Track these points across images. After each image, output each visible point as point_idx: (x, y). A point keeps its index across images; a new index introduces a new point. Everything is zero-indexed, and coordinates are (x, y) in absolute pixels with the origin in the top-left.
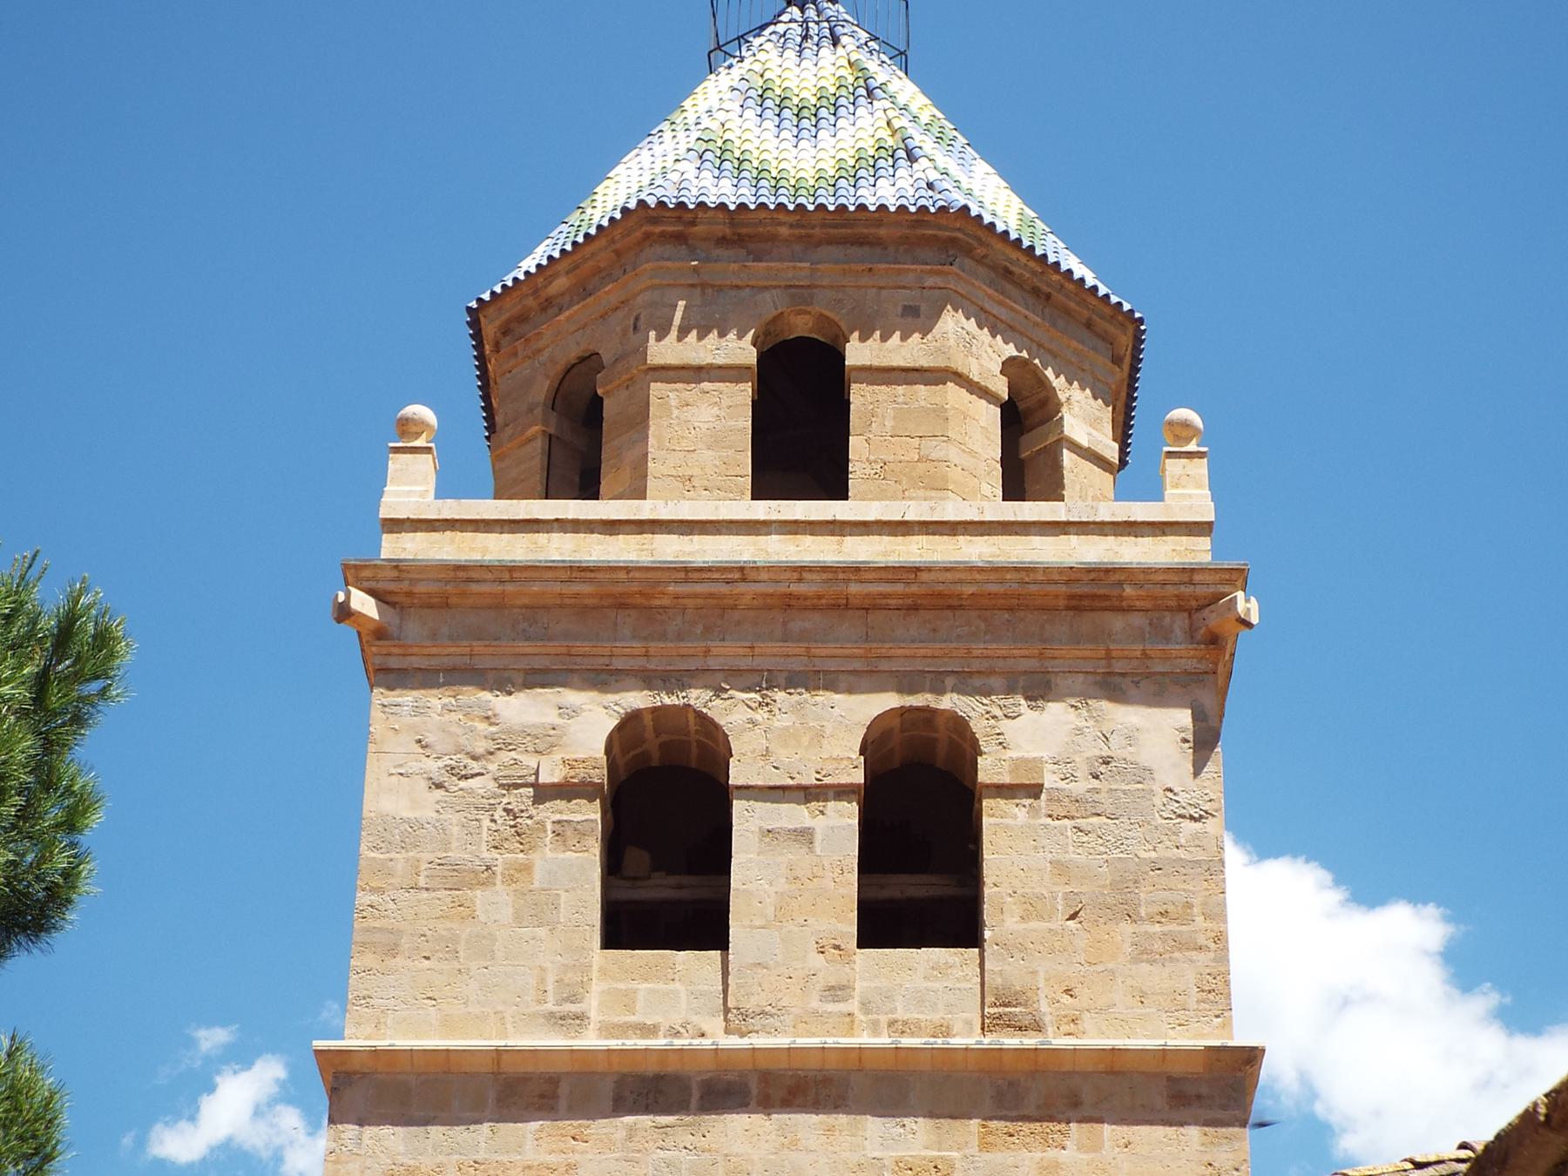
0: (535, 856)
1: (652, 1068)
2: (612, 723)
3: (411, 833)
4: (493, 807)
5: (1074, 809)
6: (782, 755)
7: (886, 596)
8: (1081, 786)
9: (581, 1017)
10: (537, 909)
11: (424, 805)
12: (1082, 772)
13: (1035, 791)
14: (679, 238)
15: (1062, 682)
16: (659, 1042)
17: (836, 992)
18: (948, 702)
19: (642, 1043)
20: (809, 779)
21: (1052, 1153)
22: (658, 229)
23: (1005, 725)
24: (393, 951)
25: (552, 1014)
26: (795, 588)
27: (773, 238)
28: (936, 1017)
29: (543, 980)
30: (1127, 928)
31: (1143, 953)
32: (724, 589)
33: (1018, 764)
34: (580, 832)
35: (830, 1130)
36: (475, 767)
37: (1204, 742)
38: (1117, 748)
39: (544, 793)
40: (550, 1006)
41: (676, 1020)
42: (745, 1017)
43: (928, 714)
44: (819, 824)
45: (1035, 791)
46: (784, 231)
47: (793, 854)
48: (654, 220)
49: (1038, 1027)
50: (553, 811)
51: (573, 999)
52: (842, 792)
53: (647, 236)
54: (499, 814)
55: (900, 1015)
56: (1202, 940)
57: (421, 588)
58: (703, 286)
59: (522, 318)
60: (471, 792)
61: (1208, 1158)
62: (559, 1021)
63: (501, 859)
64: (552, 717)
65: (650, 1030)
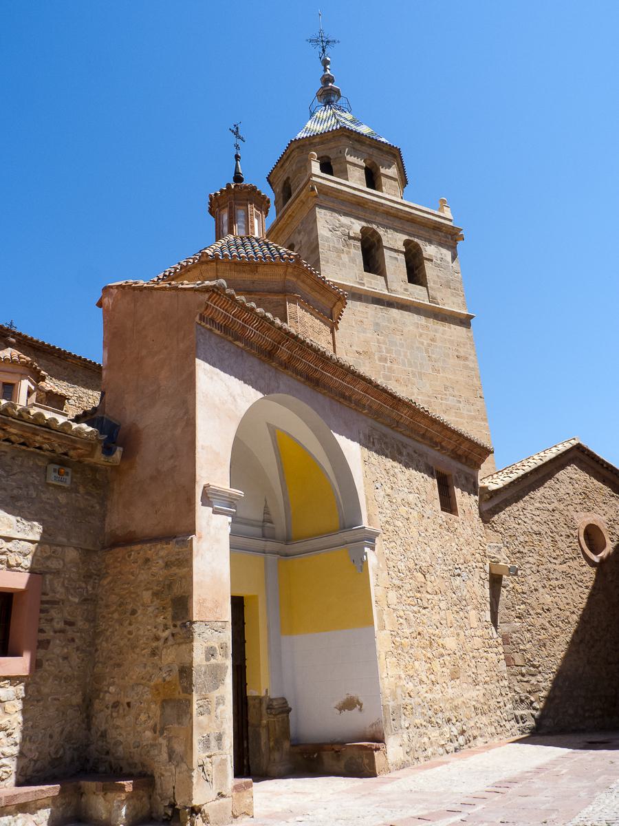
1: (377, 297)
2: (360, 228)
5: (438, 266)
7: (404, 217)
8: (439, 262)
9: (363, 284)
10: (353, 260)
11: (329, 234)
13: (432, 261)
14: (348, 137)
15: (434, 242)
17: (406, 290)
18: (416, 240)
19: (373, 290)
20: (396, 248)
24: (328, 262)
26: (391, 211)
27: (365, 143)
28: (422, 299)
32: (378, 207)
35: (409, 316)
37: (454, 258)
39: (350, 238)
40: (358, 280)
43: (412, 241)
45: (432, 261)
46: (367, 142)
47: (395, 262)
50: (352, 242)
51: (362, 280)
52: (401, 252)
57: (324, 190)
58: (354, 148)
59: (303, 146)
63: (345, 249)
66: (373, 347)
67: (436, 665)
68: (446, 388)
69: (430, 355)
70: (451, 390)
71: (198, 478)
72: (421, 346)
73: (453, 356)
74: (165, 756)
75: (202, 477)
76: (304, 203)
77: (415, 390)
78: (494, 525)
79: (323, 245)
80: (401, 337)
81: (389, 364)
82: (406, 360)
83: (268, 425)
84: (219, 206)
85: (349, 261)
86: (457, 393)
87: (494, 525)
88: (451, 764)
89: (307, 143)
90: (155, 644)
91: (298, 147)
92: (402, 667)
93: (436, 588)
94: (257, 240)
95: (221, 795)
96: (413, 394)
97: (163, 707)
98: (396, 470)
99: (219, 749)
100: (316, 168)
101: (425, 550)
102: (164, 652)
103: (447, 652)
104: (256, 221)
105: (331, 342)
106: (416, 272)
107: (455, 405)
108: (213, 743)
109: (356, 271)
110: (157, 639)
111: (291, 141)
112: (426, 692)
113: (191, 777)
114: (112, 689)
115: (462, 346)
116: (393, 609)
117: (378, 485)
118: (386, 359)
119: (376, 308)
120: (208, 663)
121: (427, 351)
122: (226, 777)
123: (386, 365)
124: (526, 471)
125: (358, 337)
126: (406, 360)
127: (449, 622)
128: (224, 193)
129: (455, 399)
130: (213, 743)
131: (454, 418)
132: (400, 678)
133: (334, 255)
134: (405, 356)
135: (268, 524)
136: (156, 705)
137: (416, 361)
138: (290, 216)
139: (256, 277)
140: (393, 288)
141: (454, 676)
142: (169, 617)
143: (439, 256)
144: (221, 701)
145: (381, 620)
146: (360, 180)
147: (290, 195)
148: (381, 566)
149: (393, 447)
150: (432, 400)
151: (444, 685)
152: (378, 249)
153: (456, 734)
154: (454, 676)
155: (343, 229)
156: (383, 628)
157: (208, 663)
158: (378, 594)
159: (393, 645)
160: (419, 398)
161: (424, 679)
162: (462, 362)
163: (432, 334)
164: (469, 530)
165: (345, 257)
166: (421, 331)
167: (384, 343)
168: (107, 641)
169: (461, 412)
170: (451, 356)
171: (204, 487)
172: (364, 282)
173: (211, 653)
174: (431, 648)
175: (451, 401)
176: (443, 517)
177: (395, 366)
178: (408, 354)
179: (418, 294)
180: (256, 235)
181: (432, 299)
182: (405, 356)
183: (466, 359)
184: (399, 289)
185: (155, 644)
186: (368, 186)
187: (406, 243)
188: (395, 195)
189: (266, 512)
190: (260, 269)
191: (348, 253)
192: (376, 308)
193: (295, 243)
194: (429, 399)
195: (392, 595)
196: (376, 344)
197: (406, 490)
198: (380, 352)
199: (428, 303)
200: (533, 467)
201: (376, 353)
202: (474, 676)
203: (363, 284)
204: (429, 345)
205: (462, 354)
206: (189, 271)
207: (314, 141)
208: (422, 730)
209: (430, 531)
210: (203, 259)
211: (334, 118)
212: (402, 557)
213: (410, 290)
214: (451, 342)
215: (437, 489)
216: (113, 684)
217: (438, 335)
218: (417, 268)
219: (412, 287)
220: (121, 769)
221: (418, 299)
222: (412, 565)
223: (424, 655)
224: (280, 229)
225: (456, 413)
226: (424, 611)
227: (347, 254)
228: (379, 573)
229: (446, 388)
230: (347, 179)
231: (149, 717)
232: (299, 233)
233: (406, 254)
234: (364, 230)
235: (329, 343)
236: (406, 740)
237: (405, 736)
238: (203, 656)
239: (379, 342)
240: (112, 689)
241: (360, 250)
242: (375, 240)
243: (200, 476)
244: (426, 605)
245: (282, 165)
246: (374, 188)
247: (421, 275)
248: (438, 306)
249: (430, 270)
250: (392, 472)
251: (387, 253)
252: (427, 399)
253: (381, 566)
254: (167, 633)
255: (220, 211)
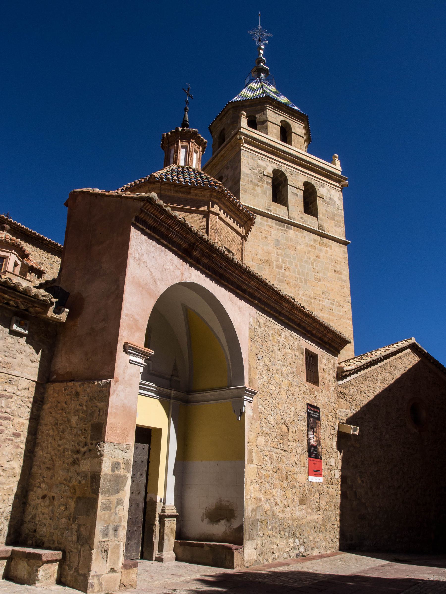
0: (264, 185)
3: (247, 175)
4: (258, 176)
5: (327, 203)
6: (294, 182)
8: (328, 200)
9: (271, 210)
10: (265, 193)
11: (249, 172)
12: (328, 198)
16: (280, 217)
17: (302, 218)
21: (327, 249)
22: (269, 101)
23: (319, 189)
24: (246, 192)
25: (267, 209)
28: (313, 225)
29: (266, 203)
30: (334, 221)
31: (335, 226)
33: (322, 195)
34: (269, 183)
36: (255, 169)
38: (332, 196)
40: (267, 207)
41: (282, 215)
42: (291, 217)
44: (298, 193)
45: (323, 198)
47: (295, 197)
48: (269, 99)
49: (324, 231)
50: (265, 179)
51: (269, 207)
53: (267, 101)
54: (259, 177)
55: (309, 224)
56: (342, 226)
59: (237, 106)
60: (254, 172)
61: (343, 255)
62: (269, 210)
63: (260, 184)
64: (265, 166)
65: (279, 215)
66: (273, 258)
67: (290, 493)
68: (324, 293)
69: (315, 267)
70: (327, 294)
71: (120, 337)
72: (309, 260)
73: (331, 270)
74: (75, 538)
75: (123, 337)
76: (233, 147)
77: (301, 292)
78: (345, 396)
79: (244, 179)
80: (295, 252)
81: (283, 271)
82: (296, 269)
83: (182, 304)
84: (169, 143)
85: (262, 193)
86: (332, 298)
87: (345, 396)
88: (291, 565)
89: (241, 104)
90: (75, 456)
91: (233, 108)
92: (263, 492)
93: (296, 438)
94: (194, 170)
95: (113, 570)
96: (298, 295)
97: (77, 502)
98: (275, 348)
99: (115, 536)
100: (244, 122)
101: (290, 409)
102: (82, 462)
103: (298, 485)
104: (195, 155)
105: (240, 250)
106: (311, 206)
107: (329, 306)
108: (111, 532)
109: (266, 201)
110: (78, 452)
111: (229, 102)
112: (279, 512)
113: (91, 555)
114: (43, 485)
115: (339, 263)
116: (261, 449)
117: (260, 357)
118: (281, 268)
119: (278, 229)
120: (113, 474)
121: (312, 264)
122: (118, 558)
123: (281, 271)
124: (373, 359)
125: (263, 249)
126: (296, 269)
127: (302, 464)
128: (173, 134)
129: (330, 301)
130: (111, 532)
131: (327, 316)
132: (260, 500)
133: (252, 186)
134: (296, 266)
135: (175, 378)
136: (72, 499)
137: (304, 271)
138: (222, 156)
139: (189, 197)
140: (292, 216)
141: (302, 502)
142: (89, 438)
143: (329, 196)
144: (119, 502)
145: (250, 456)
146: (276, 135)
147: (224, 141)
148: (255, 417)
149: (274, 330)
150: (312, 301)
151: (294, 508)
152: (284, 187)
153: (298, 544)
154: (302, 502)
155: (260, 169)
156: (251, 462)
157: (113, 474)
158: (251, 437)
159: (258, 475)
160: (303, 298)
161: (279, 502)
162: (337, 275)
163: (317, 252)
164: (326, 399)
165: (259, 190)
166: (310, 249)
167: (281, 255)
168: (42, 450)
169: (333, 311)
170: (330, 270)
171: (124, 345)
172: (271, 209)
173: (116, 466)
174: (286, 480)
175: (326, 303)
176: (307, 386)
177: (287, 273)
178: (298, 265)
179: (311, 223)
180: (194, 166)
181: (320, 227)
182: (296, 266)
183: (341, 273)
184: (296, 217)
185: (75, 456)
186: (282, 140)
187: (306, 184)
188: (301, 149)
189: (175, 369)
190: (192, 191)
191: (262, 187)
192: (278, 229)
193: (223, 176)
194: (310, 300)
195: (261, 440)
196: (275, 255)
197: (281, 363)
198: (278, 261)
199: (318, 230)
200: (378, 357)
201: (275, 262)
202: (317, 504)
203: (270, 211)
204: (315, 260)
205: (338, 269)
206: (140, 188)
207: (246, 104)
208: (273, 539)
209: (296, 395)
210: (151, 180)
211: (262, 89)
212: (272, 412)
213: (304, 218)
214: (332, 260)
215: (305, 365)
216: (43, 482)
217: (322, 254)
218: (311, 203)
219: (306, 216)
220: (43, 543)
221: (309, 225)
222: (279, 419)
223: (281, 485)
224: (214, 165)
225: (329, 312)
226: (284, 453)
227: (261, 187)
228: (253, 422)
229: (324, 293)
230: (267, 134)
231: (66, 508)
232: (227, 168)
233: (304, 192)
234: (275, 172)
235: (238, 250)
236: (259, 546)
237: (259, 542)
238: (110, 469)
239: (277, 254)
240: (43, 485)
241: (271, 185)
242: (282, 179)
243: (122, 335)
244: (286, 449)
245: (221, 119)
246: (286, 142)
247: (314, 208)
248: (324, 232)
249: (321, 206)
250: (271, 349)
251: (291, 190)
252: (308, 299)
253: (255, 417)
254: (86, 448)
255: (169, 146)
